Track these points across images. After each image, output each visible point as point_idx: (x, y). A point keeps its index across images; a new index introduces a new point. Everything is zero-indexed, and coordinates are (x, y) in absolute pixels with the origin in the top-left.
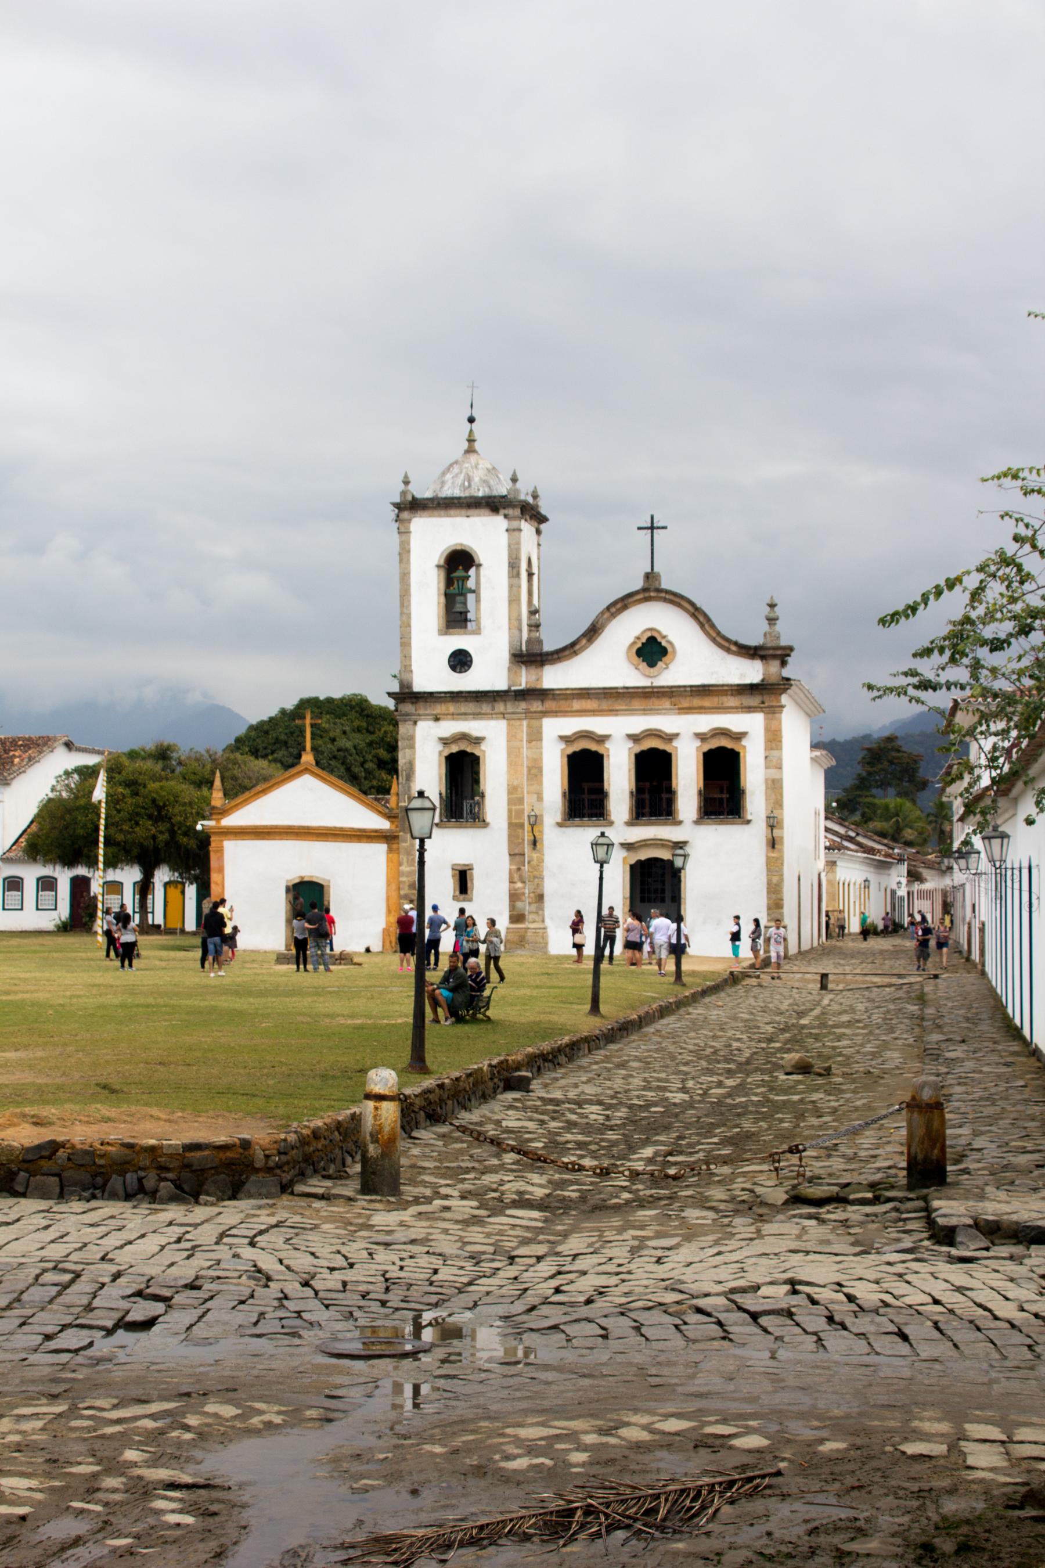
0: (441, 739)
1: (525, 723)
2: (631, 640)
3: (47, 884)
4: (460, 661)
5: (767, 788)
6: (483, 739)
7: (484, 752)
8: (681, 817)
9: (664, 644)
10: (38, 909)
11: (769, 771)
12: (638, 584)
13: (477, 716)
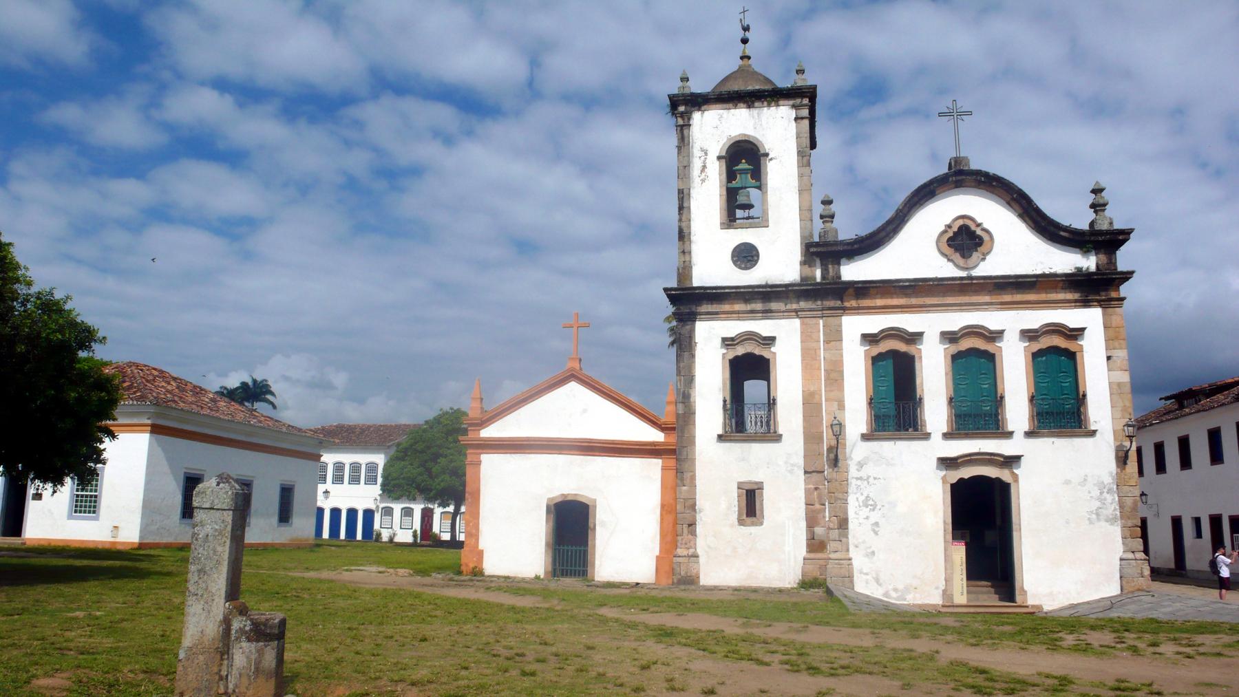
0: (724, 340)
1: (821, 322)
2: (943, 228)
3: (408, 512)
4: (746, 256)
5: (1111, 394)
6: (773, 339)
7: (775, 353)
8: (1010, 427)
9: (979, 232)
10: (401, 528)
11: (1110, 372)
12: (945, 170)
13: (767, 314)
